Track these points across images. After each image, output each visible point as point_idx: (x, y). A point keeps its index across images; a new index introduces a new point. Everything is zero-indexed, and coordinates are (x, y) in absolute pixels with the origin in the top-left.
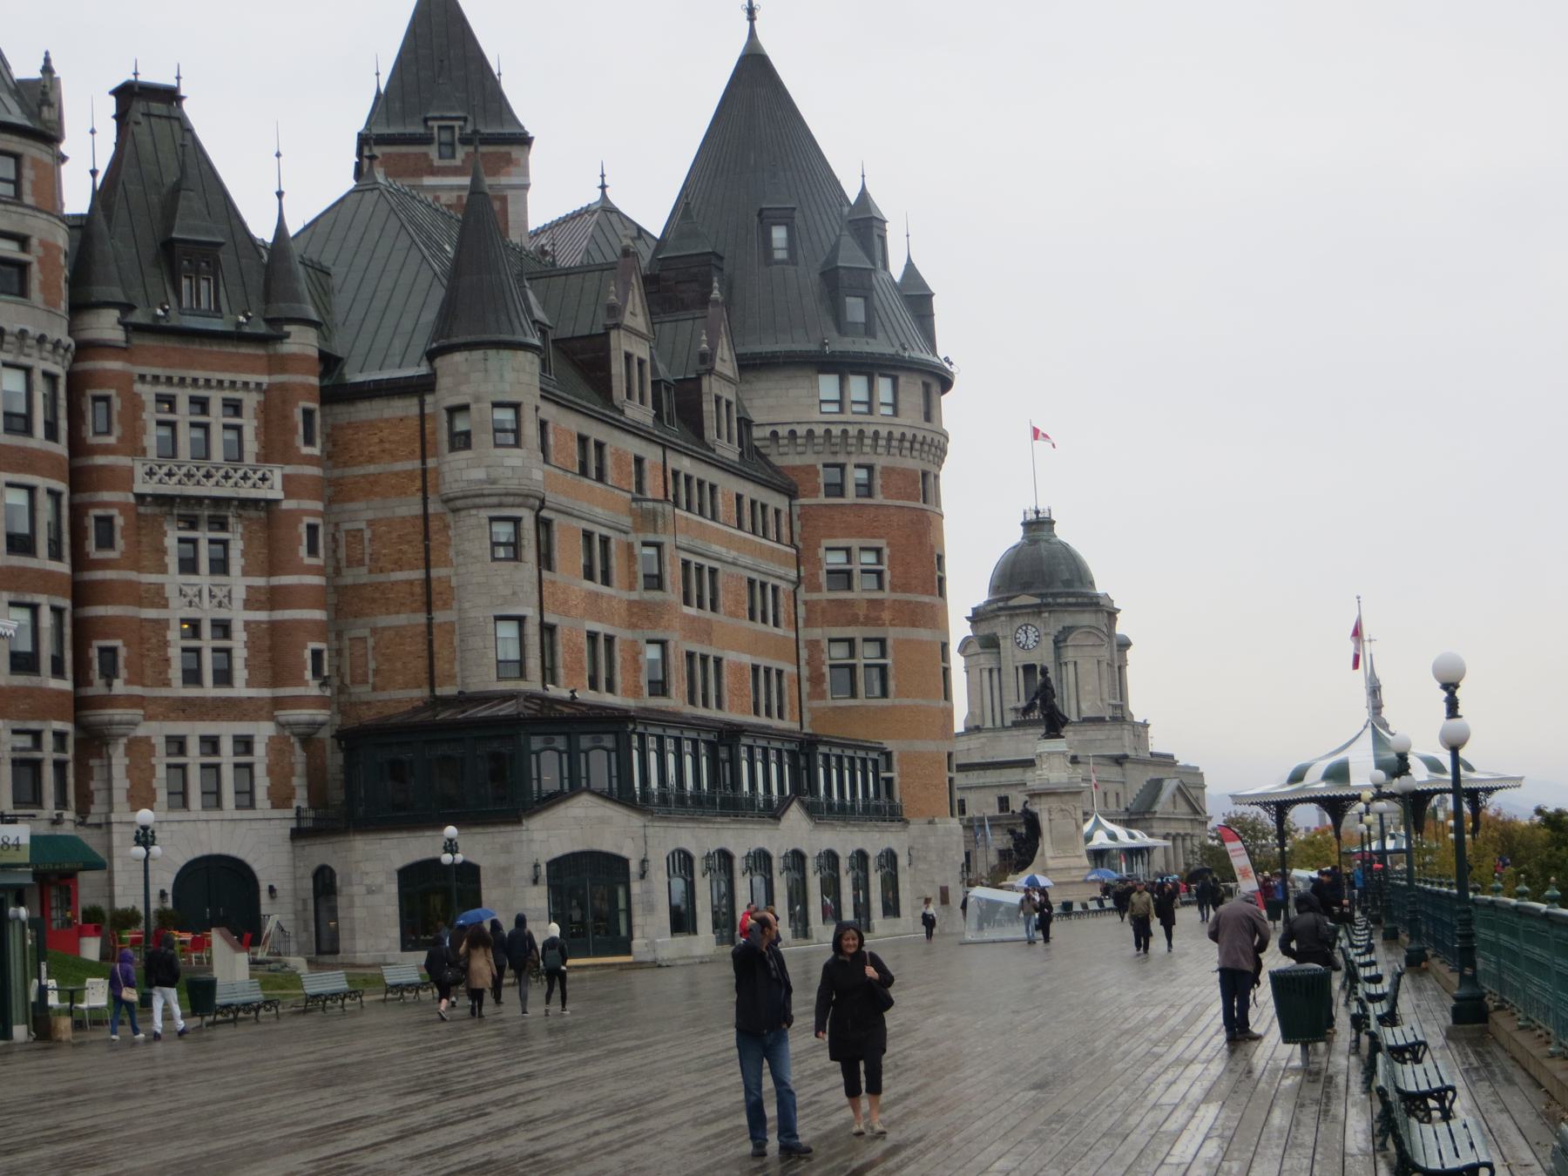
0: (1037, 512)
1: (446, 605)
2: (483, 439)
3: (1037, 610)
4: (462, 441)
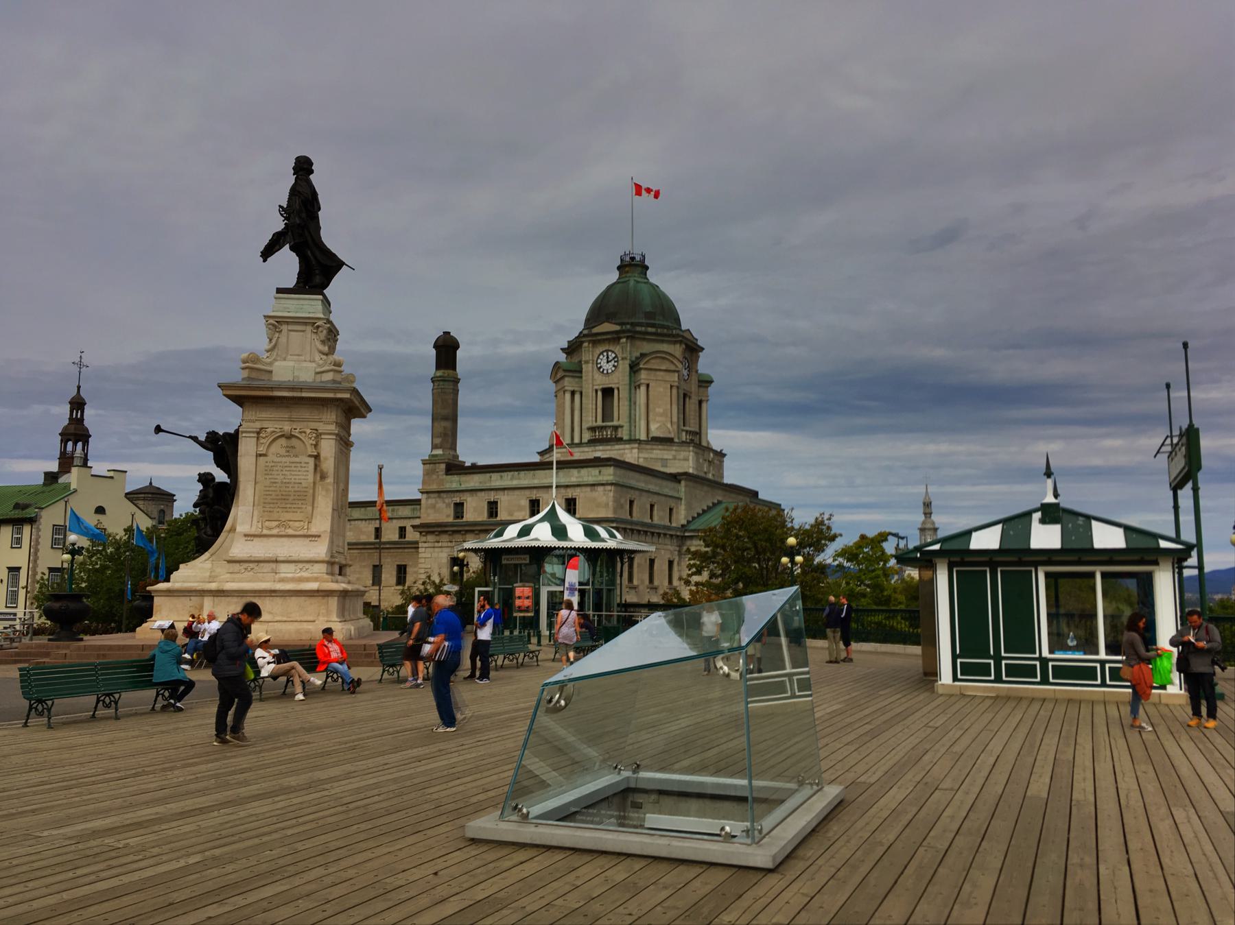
0: (633, 259)
3: (614, 338)
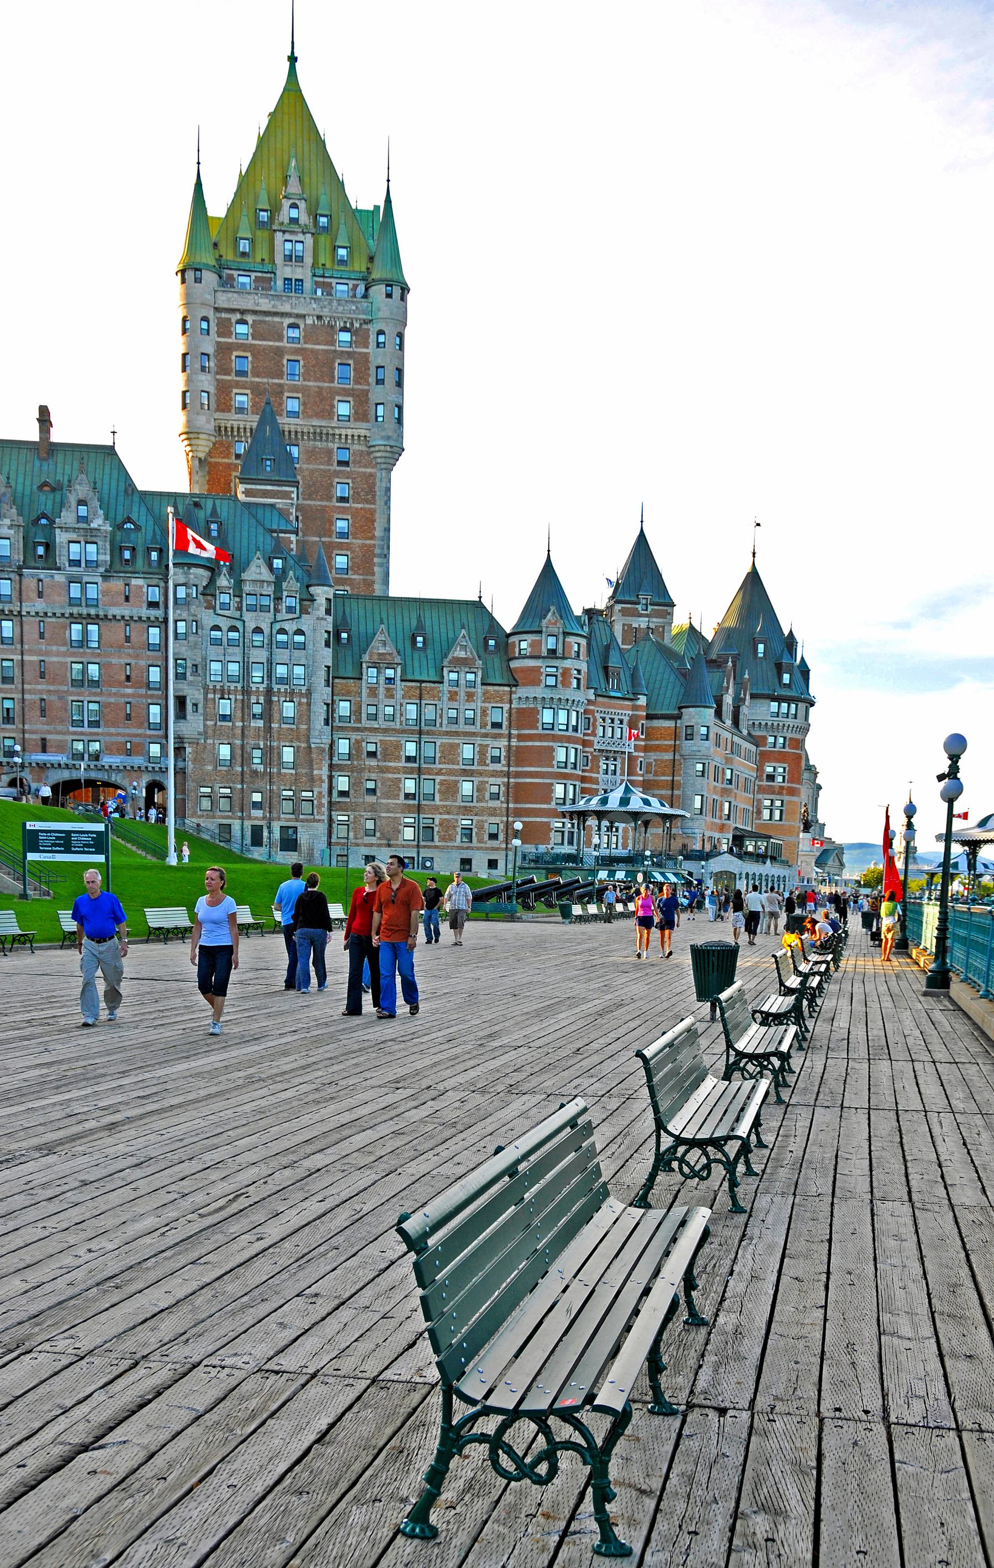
1: (679, 789)
2: (697, 738)
4: (690, 737)
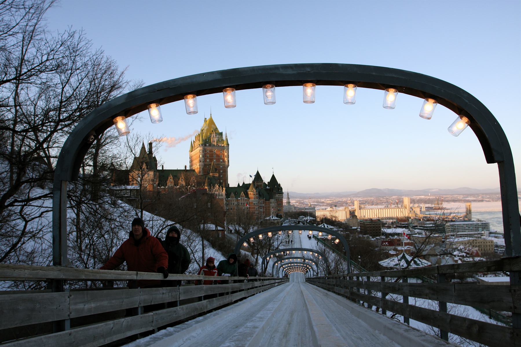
4: (271, 203)
